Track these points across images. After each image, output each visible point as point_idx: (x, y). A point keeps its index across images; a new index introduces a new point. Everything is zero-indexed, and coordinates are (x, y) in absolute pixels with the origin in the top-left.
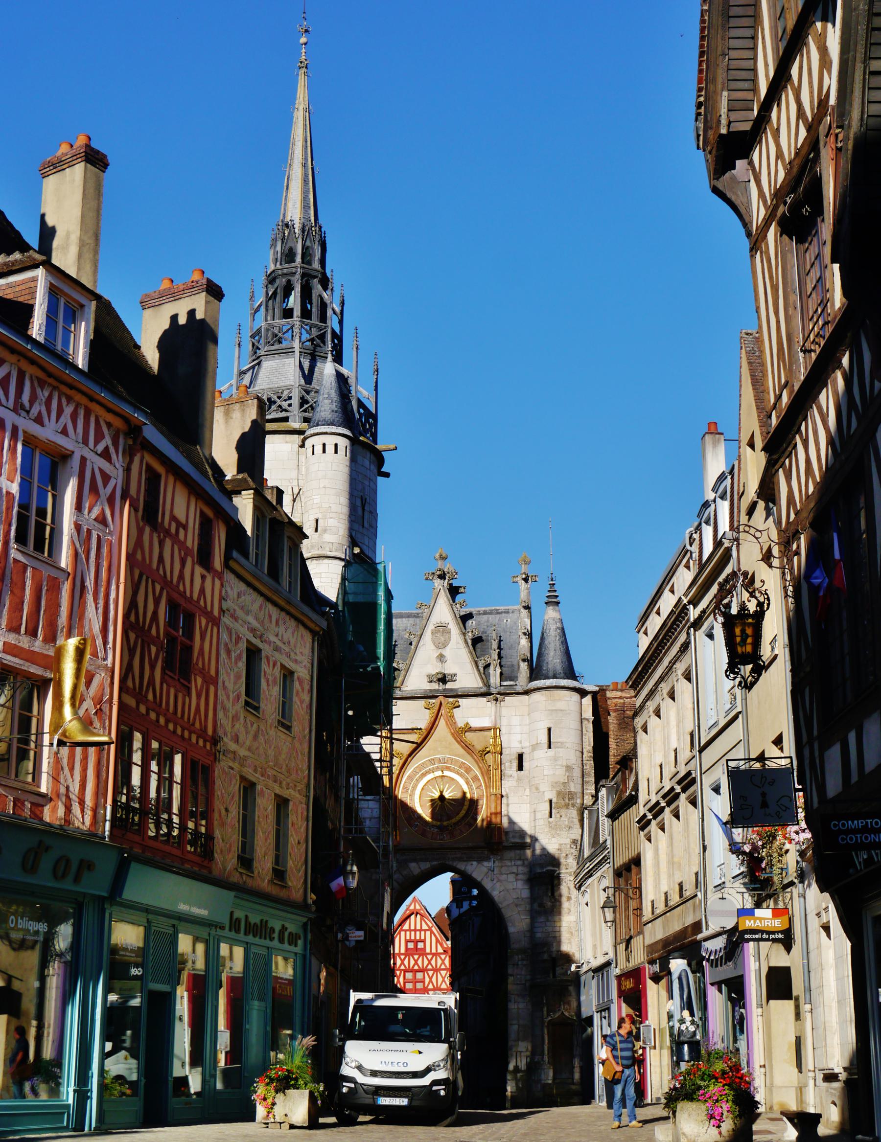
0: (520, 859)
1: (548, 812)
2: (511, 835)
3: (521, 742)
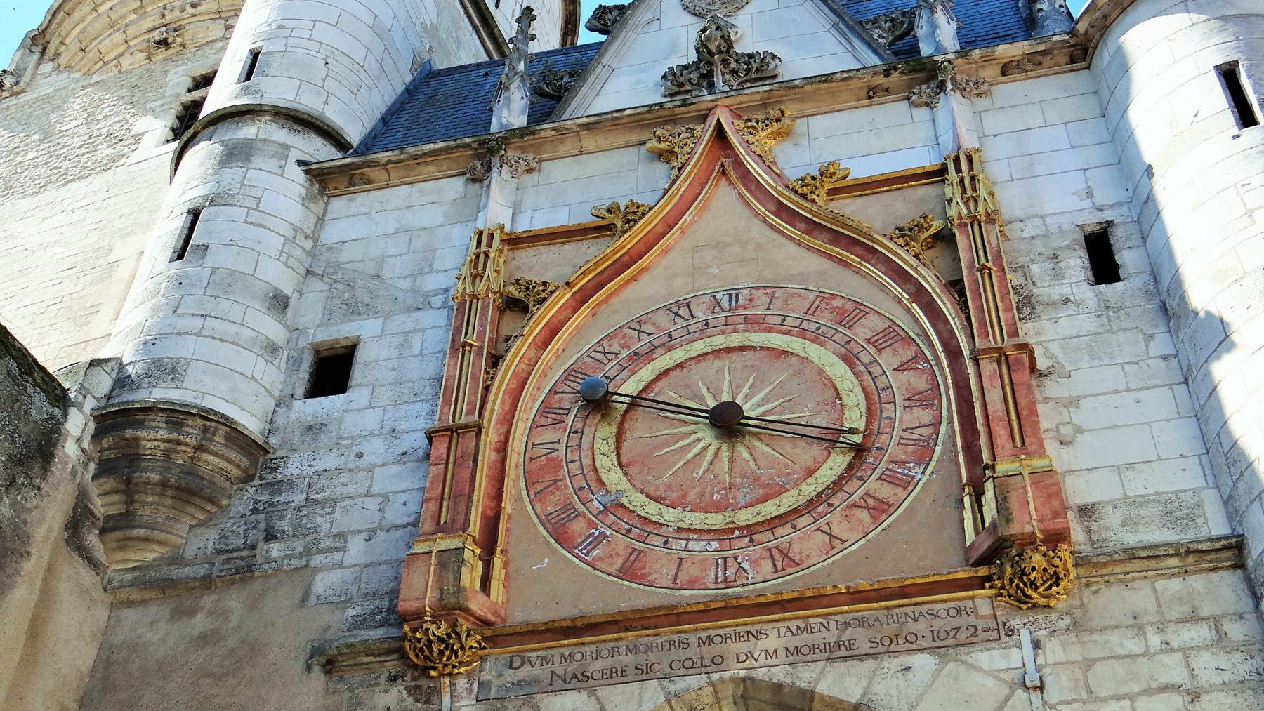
0: (1194, 618)
2: (1113, 518)
3: (1089, 194)
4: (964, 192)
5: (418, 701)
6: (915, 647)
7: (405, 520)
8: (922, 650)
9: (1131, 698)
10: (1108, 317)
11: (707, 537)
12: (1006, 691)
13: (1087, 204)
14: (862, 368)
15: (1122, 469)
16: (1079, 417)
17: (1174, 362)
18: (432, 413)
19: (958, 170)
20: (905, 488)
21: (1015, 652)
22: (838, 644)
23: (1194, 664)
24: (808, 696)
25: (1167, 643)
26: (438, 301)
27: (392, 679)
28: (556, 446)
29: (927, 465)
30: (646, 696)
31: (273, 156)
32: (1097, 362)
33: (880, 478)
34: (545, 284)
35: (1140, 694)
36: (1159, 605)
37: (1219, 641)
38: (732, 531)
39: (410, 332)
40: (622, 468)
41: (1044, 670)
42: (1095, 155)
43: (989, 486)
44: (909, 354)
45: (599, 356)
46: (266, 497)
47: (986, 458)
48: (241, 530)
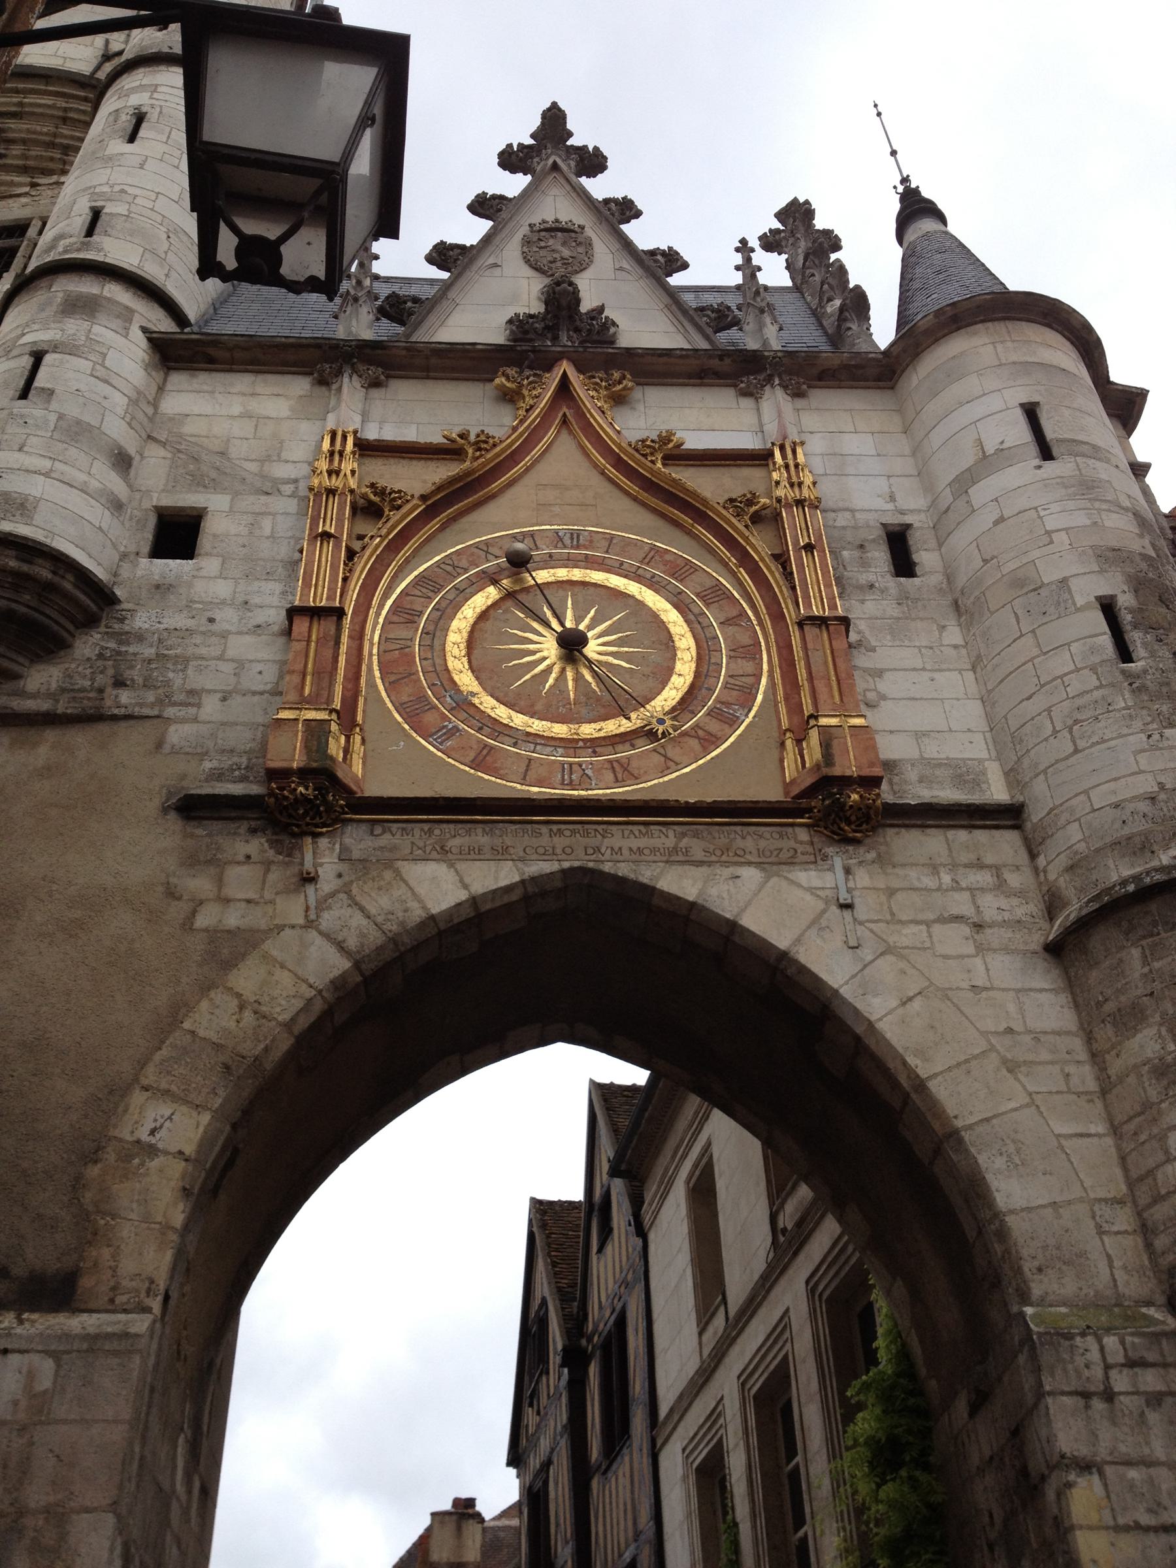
0: (979, 865)
1: (1106, 641)
2: (912, 775)
3: (892, 498)
4: (789, 477)
5: (280, 854)
6: (743, 860)
7: (261, 688)
8: (750, 863)
9: (928, 924)
10: (908, 606)
11: (553, 743)
12: (821, 905)
13: (890, 506)
14: (692, 617)
15: (919, 735)
16: (883, 686)
17: (964, 651)
18: (284, 593)
19: (784, 457)
20: (731, 726)
21: (829, 876)
22: (675, 850)
23: (979, 902)
24: (650, 891)
25: (957, 882)
26: (288, 489)
27: (253, 831)
28: (409, 643)
29: (750, 711)
30: (502, 874)
31: (118, 317)
32: (898, 643)
33: (708, 714)
34: (400, 491)
35: (934, 921)
36: (950, 850)
37: (1000, 886)
38: (578, 741)
39: (262, 514)
40: (473, 672)
41: (854, 893)
42: (906, 465)
43: (814, 734)
44: (735, 613)
45: (449, 568)
46: (112, 645)
47: (808, 709)
48: (88, 671)
